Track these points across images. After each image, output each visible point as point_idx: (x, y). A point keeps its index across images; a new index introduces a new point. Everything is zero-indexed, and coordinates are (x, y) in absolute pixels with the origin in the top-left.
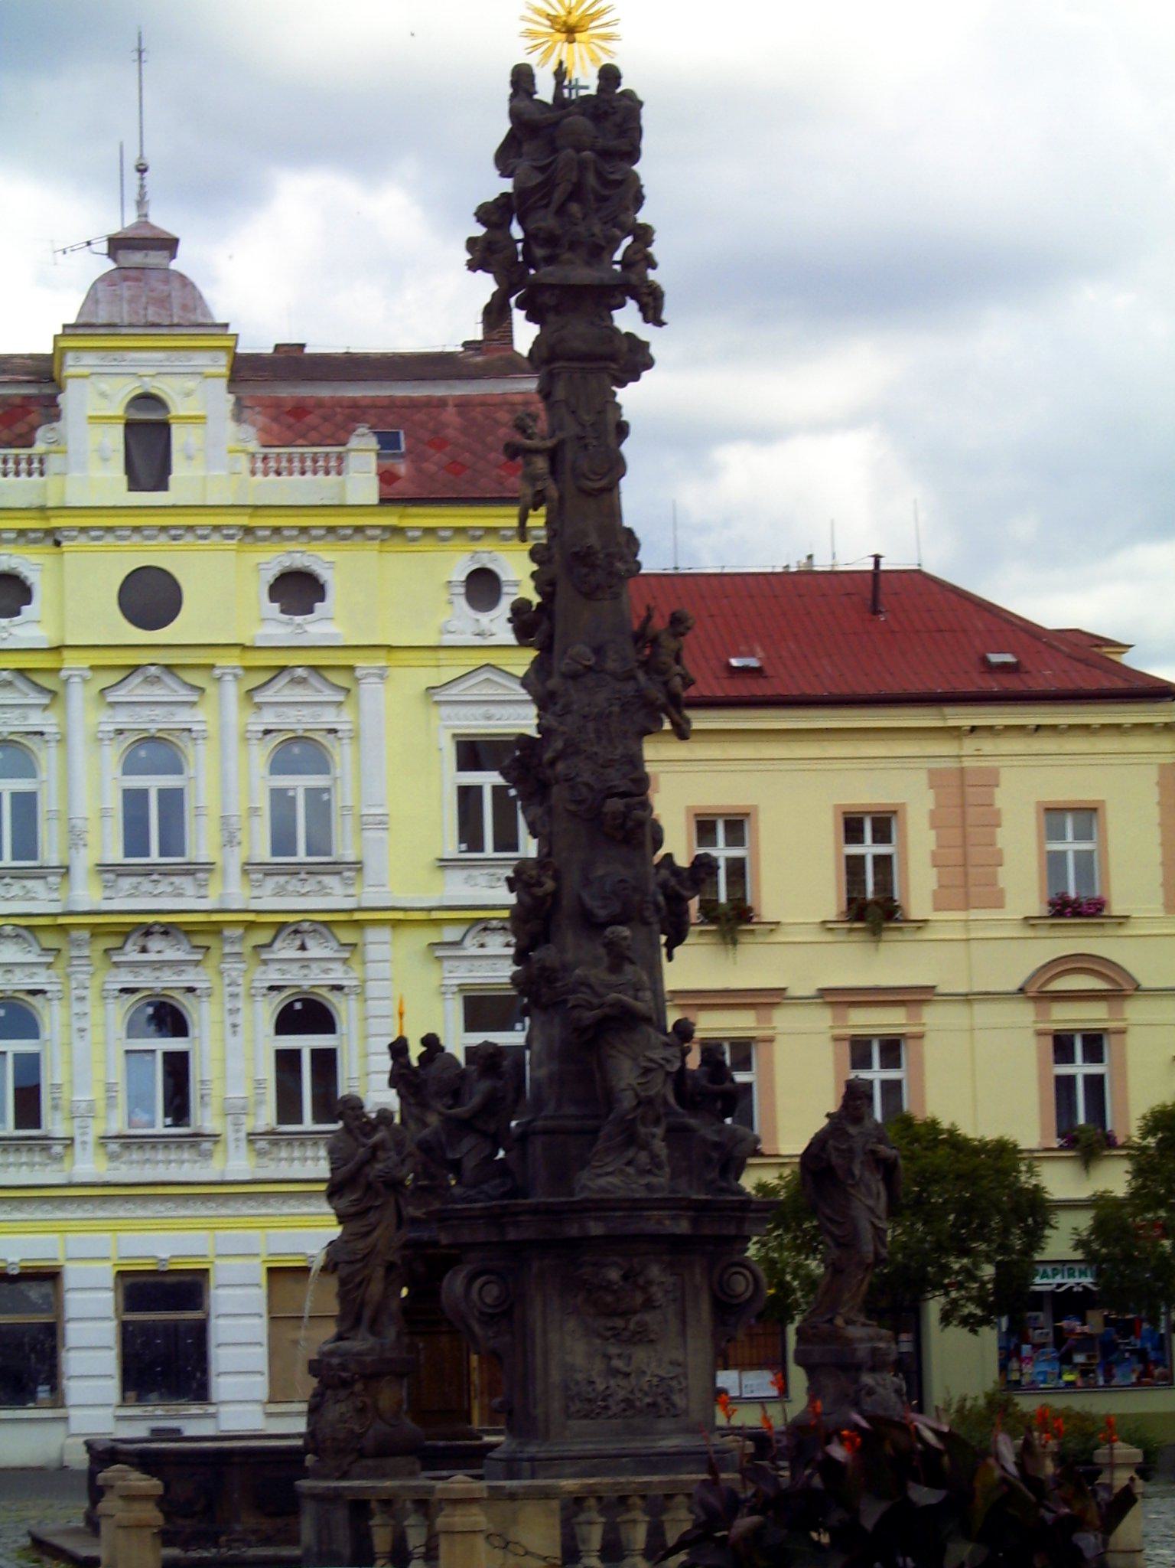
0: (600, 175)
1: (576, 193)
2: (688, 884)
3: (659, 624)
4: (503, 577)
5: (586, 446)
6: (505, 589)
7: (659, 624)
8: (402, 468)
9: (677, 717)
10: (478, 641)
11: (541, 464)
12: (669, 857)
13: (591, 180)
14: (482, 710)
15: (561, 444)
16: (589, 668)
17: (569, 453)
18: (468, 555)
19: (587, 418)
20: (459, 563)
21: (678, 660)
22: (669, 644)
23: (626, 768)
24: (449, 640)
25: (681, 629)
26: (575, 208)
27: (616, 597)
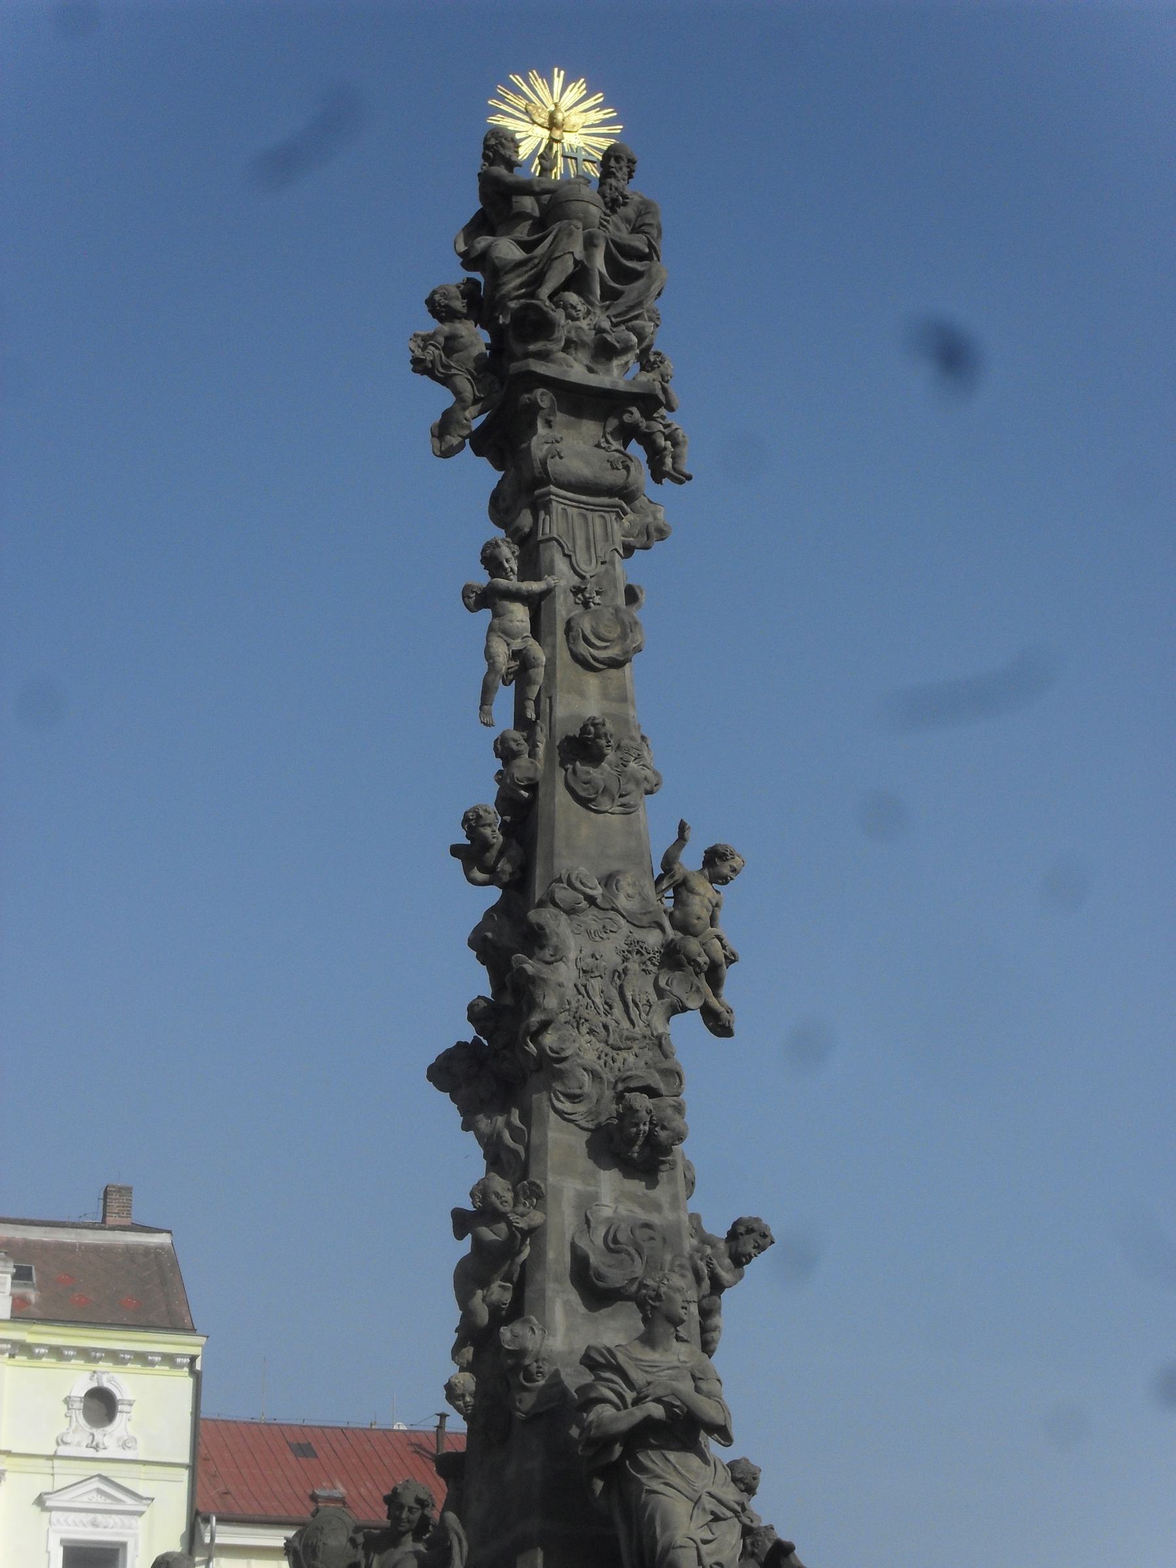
0: (609, 259)
1: (578, 280)
2: (727, 1261)
3: (691, 861)
4: (119, 1397)
5: (586, 604)
6: (120, 1408)
7: (691, 861)
8: (33, 1296)
9: (713, 1002)
10: (91, 1453)
11: (519, 614)
12: (695, 1218)
13: (599, 263)
14: (91, 1516)
15: (548, 592)
16: (591, 900)
17: (563, 607)
18: (88, 1375)
19: (583, 567)
20: (79, 1380)
21: (713, 921)
22: (704, 888)
23: (649, 1055)
24: (63, 1451)
25: (726, 870)
26: (573, 298)
27: (628, 810)
